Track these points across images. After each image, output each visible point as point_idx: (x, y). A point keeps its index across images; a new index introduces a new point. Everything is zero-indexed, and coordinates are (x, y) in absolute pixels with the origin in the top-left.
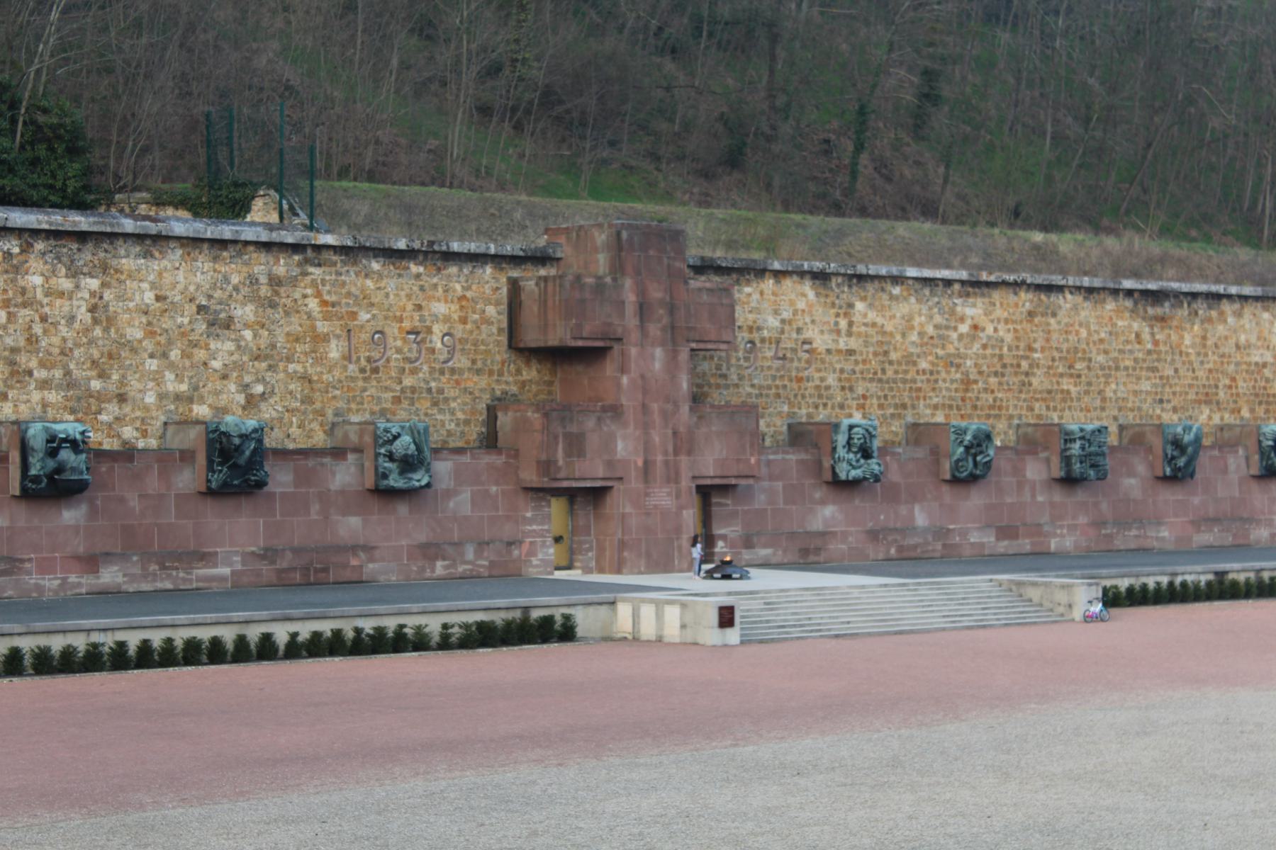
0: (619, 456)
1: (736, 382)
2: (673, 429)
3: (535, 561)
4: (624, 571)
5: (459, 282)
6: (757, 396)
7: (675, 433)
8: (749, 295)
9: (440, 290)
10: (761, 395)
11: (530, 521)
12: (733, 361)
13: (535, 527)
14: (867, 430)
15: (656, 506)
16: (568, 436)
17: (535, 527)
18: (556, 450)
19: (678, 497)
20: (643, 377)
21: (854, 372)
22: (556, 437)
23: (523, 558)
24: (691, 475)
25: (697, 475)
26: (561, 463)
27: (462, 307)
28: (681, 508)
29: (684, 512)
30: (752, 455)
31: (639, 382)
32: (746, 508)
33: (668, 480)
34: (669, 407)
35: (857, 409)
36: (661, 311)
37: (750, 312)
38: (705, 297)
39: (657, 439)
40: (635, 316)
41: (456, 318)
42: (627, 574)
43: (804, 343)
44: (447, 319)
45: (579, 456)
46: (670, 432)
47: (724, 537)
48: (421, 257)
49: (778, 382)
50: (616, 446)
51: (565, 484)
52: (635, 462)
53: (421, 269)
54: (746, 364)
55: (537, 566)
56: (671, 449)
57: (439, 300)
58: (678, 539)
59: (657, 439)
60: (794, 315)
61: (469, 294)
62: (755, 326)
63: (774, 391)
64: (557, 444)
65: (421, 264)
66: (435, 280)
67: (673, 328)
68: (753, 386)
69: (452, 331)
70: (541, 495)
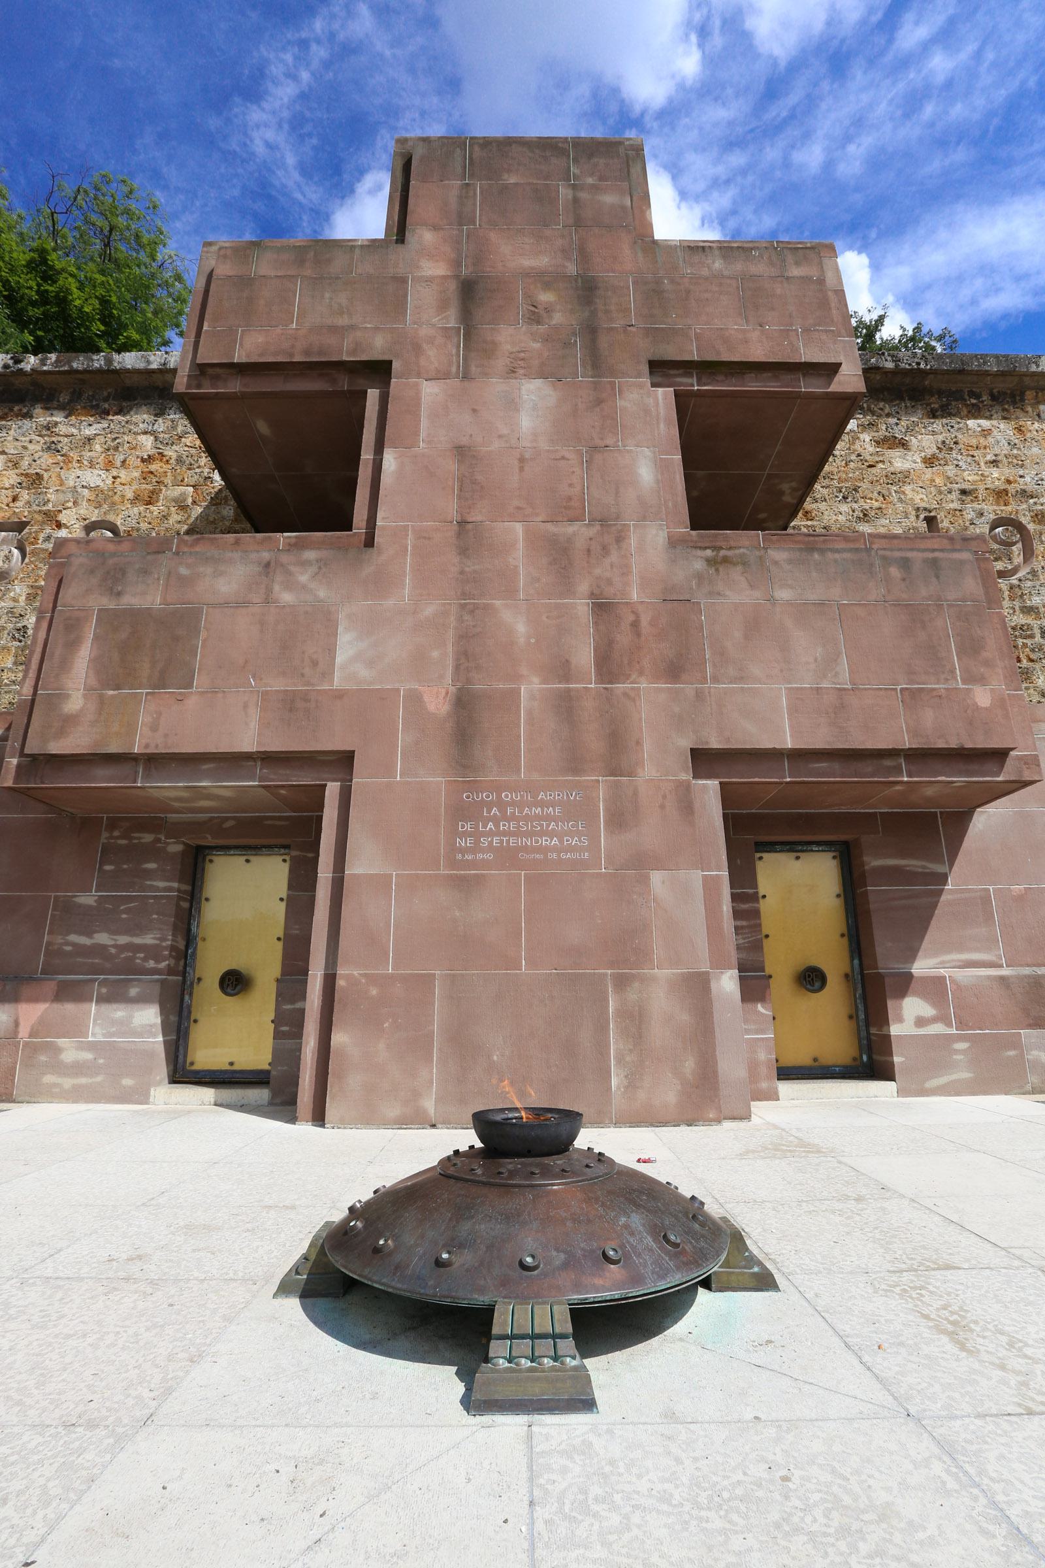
0: (338, 682)
2: (592, 595)
3: (70, 1052)
4: (332, 1110)
5: (153, 433)
7: (602, 608)
8: (986, 433)
9: (98, 447)
11: (88, 920)
13: (103, 938)
15: (508, 857)
16: (110, 620)
17: (103, 938)
18: (65, 665)
19: (619, 820)
20: (462, 452)
22: (73, 627)
23: (24, 1032)
24: (685, 743)
25: (715, 744)
26: (75, 703)
27: (146, 476)
28: (642, 863)
29: (657, 878)
30: (970, 678)
31: (450, 466)
32: (1017, 888)
33: (574, 763)
34: (580, 532)
36: (546, 297)
37: (995, 463)
38: (718, 264)
39: (521, 628)
40: (443, 306)
41: (130, 495)
42: (343, 1123)
44: (100, 497)
45: (160, 682)
46: (582, 607)
47: (935, 989)
48: (64, 398)
50: (331, 650)
51: (102, 780)
52: (415, 699)
53: (58, 417)
55: (78, 1069)
56: (584, 656)
57: (92, 465)
58: (622, 983)
59: (521, 628)
61: (170, 452)
62: (1012, 489)
64: (73, 645)
65: (61, 408)
66: (88, 432)
67: (591, 331)
69: (111, 518)
70: (148, 838)
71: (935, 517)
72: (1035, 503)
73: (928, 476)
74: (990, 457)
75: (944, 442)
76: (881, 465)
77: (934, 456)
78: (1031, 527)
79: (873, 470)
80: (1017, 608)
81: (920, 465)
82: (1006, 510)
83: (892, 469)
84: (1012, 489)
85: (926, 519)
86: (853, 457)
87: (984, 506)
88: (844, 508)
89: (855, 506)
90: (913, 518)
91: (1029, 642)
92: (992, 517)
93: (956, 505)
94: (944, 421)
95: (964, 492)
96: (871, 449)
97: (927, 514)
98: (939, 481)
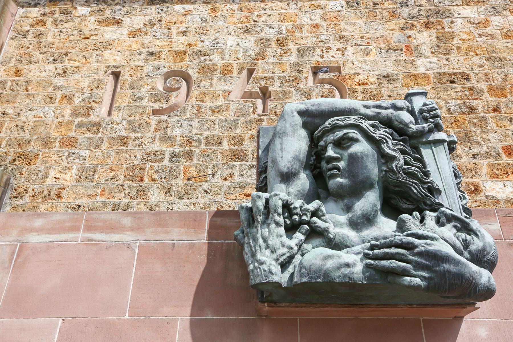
1: (123, 133)
6: (174, 157)
10: (189, 155)
12: (123, 101)
14: (388, 123)
21: (472, 110)
35: (495, 176)
43: (316, 71)
49: (238, 131)
54: (157, 106)
60: (289, 32)
63: (226, 146)
68: (164, 139)
71: (120, 72)
72: (205, 60)
73: (128, 44)
74: (182, 29)
75: (151, 20)
76: (94, 37)
77: (139, 30)
78: (195, 77)
79: (86, 41)
80: (157, 138)
81: (126, 36)
82: (178, 66)
83: (101, 40)
84: (189, 50)
85: (113, 73)
86: (75, 32)
87: (163, 63)
88: (51, 67)
89: (60, 66)
90: (101, 73)
91: (156, 165)
92: (166, 70)
93: (141, 63)
94: (158, 6)
95: (152, 54)
96: (92, 27)
97: (115, 70)
98: (134, 47)
